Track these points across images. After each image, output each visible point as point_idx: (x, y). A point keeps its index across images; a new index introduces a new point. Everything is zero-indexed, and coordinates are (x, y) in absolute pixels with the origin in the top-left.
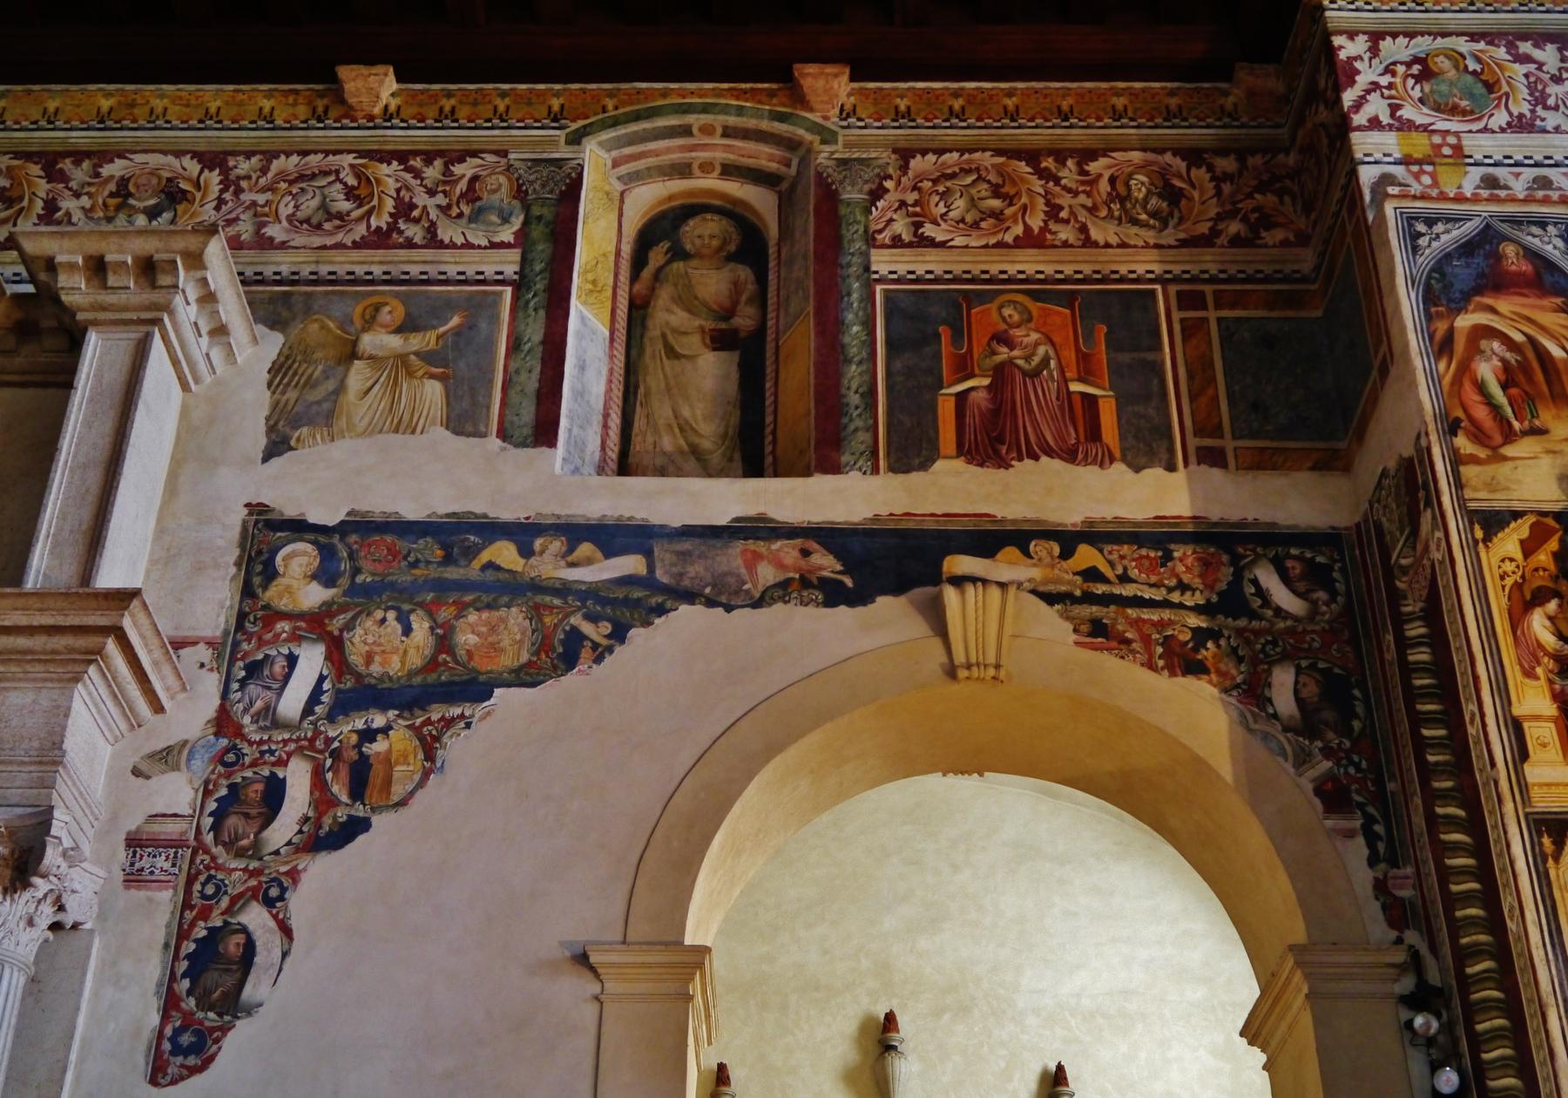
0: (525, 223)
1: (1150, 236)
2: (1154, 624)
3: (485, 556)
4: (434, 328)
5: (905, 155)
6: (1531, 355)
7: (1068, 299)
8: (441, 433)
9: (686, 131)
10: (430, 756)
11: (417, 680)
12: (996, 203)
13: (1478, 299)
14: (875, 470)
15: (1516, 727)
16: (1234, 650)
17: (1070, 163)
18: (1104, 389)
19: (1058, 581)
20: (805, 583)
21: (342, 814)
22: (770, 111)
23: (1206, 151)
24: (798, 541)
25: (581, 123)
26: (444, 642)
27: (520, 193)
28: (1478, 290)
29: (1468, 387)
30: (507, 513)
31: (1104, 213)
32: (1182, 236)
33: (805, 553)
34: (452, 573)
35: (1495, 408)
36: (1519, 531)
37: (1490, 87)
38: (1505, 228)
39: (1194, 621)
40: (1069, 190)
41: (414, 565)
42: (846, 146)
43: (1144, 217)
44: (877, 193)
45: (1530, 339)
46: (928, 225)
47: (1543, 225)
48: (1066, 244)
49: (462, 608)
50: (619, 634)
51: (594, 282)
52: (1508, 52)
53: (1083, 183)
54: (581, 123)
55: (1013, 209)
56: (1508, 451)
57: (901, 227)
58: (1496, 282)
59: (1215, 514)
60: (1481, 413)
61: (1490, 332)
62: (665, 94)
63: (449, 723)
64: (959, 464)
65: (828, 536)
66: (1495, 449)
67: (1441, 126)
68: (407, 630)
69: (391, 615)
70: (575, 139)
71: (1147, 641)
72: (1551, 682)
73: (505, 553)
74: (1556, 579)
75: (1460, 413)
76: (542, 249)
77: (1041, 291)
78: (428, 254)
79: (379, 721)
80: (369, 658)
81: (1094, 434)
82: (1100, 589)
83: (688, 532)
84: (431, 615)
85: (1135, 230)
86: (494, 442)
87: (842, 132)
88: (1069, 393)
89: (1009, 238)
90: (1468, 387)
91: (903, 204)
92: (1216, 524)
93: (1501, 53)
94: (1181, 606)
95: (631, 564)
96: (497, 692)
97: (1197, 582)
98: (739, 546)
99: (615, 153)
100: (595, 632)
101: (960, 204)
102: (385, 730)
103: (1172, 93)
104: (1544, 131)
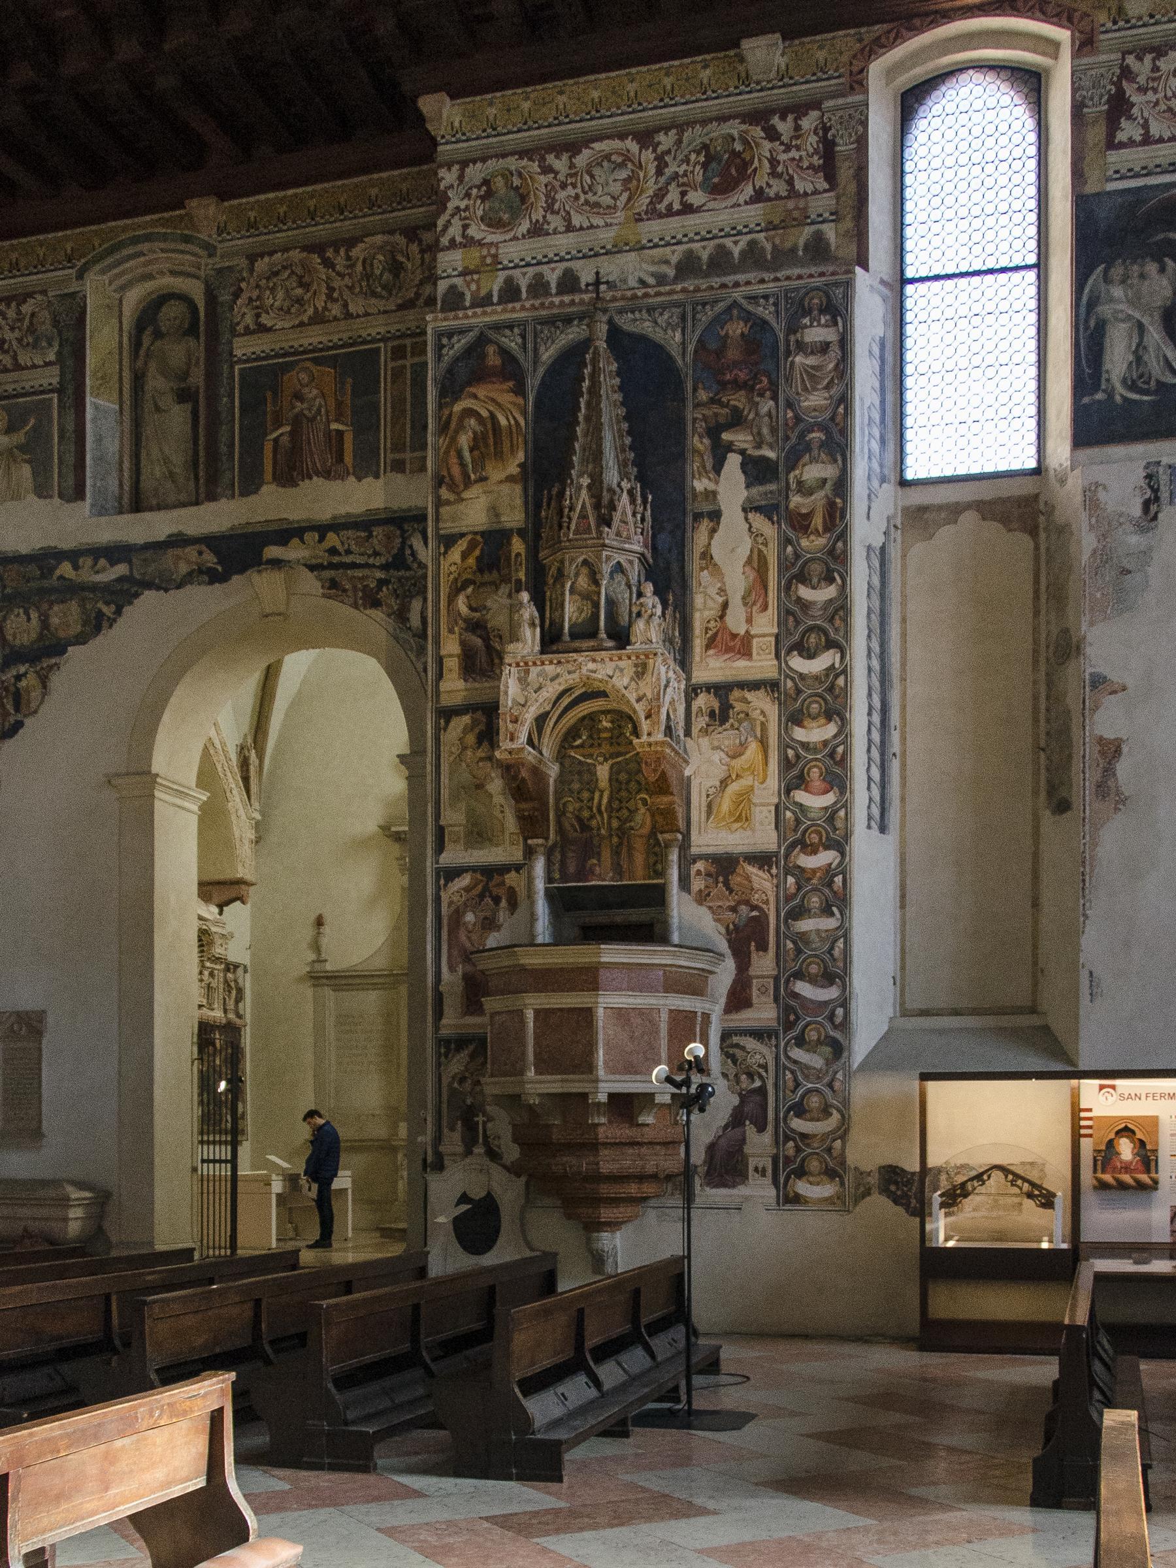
0: (61, 345)
1: (381, 304)
2: (360, 579)
3: (58, 572)
4: (22, 428)
5: (252, 258)
6: (489, 426)
7: (333, 361)
8: (32, 498)
10: (45, 687)
11: (35, 646)
12: (299, 291)
14: (233, 497)
15: (440, 661)
16: (395, 590)
17: (342, 251)
18: (346, 425)
19: (316, 557)
20: (200, 571)
21: (12, 720)
22: (181, 235)
23: (417, 227)
24: (197, 547)
25: (83, 261)
26: (45, 623)
27: (56, 323)
28: (469, 383)
29: (453, 453)
30: (66, 545)
31: (357, 290)
32: (400, 301)
33: (200, 553)
34: (46, 583)
35: (463, 465)
36: (462, 545)
37: (523, 198)
38: (492, 334)
39: (380, 575)
40: (339, 274)
41: (28, 581)
42: (222, 257)
43: (379, 289)
44: (237, 294)
45: (493, 416)
46: (264, 315)
47: (511, 328)
48: (336, 319)
49: (51, 604)
50: (119, 612)
51: (102, 378)
52: (540, 166)
53: (348, 267)
54: (83, 261)
55: (309, 294)
56: (465, 495)
57: (249, 320)
58: (480, 375)
59: (395, 506)
60: (456, 471)
61: (469, 412)
62: (124, 229)
63: (51, 668)
64: (273, 487)
65: (210, 541)
66: (458, 494)
67: (490, 238)
68: (29, 619)
69: (21, 611)
70: (80, 276)
71: (355, 588)
72: (460, 634)
73: (65, 569)
74: (474, 573)
75: (445, 473)
76: (70, 362)
77: (320, 357)
78: (14, 375)
79: (22, 669)
80: (15, 637)
81: (340, 459)
82: (336, 559)
83: (147, 546)
84: (38, 608)
85: (373, 301)
86: (57, 501)
87: (219, 246)
88: (330, 431)
89: (305, 319)
90: (453, 453)
91: (250, 299)
92: (395, 512)
93: (535, 167)
94: (374, 566)
95: (121, 569)
96: (69, 648)
97: (383, 550)
98: (170, 552)
100: (108, 610)
101: (280, 295)
102: (25, 674)
103: (404, 179)
104: (548, 234)
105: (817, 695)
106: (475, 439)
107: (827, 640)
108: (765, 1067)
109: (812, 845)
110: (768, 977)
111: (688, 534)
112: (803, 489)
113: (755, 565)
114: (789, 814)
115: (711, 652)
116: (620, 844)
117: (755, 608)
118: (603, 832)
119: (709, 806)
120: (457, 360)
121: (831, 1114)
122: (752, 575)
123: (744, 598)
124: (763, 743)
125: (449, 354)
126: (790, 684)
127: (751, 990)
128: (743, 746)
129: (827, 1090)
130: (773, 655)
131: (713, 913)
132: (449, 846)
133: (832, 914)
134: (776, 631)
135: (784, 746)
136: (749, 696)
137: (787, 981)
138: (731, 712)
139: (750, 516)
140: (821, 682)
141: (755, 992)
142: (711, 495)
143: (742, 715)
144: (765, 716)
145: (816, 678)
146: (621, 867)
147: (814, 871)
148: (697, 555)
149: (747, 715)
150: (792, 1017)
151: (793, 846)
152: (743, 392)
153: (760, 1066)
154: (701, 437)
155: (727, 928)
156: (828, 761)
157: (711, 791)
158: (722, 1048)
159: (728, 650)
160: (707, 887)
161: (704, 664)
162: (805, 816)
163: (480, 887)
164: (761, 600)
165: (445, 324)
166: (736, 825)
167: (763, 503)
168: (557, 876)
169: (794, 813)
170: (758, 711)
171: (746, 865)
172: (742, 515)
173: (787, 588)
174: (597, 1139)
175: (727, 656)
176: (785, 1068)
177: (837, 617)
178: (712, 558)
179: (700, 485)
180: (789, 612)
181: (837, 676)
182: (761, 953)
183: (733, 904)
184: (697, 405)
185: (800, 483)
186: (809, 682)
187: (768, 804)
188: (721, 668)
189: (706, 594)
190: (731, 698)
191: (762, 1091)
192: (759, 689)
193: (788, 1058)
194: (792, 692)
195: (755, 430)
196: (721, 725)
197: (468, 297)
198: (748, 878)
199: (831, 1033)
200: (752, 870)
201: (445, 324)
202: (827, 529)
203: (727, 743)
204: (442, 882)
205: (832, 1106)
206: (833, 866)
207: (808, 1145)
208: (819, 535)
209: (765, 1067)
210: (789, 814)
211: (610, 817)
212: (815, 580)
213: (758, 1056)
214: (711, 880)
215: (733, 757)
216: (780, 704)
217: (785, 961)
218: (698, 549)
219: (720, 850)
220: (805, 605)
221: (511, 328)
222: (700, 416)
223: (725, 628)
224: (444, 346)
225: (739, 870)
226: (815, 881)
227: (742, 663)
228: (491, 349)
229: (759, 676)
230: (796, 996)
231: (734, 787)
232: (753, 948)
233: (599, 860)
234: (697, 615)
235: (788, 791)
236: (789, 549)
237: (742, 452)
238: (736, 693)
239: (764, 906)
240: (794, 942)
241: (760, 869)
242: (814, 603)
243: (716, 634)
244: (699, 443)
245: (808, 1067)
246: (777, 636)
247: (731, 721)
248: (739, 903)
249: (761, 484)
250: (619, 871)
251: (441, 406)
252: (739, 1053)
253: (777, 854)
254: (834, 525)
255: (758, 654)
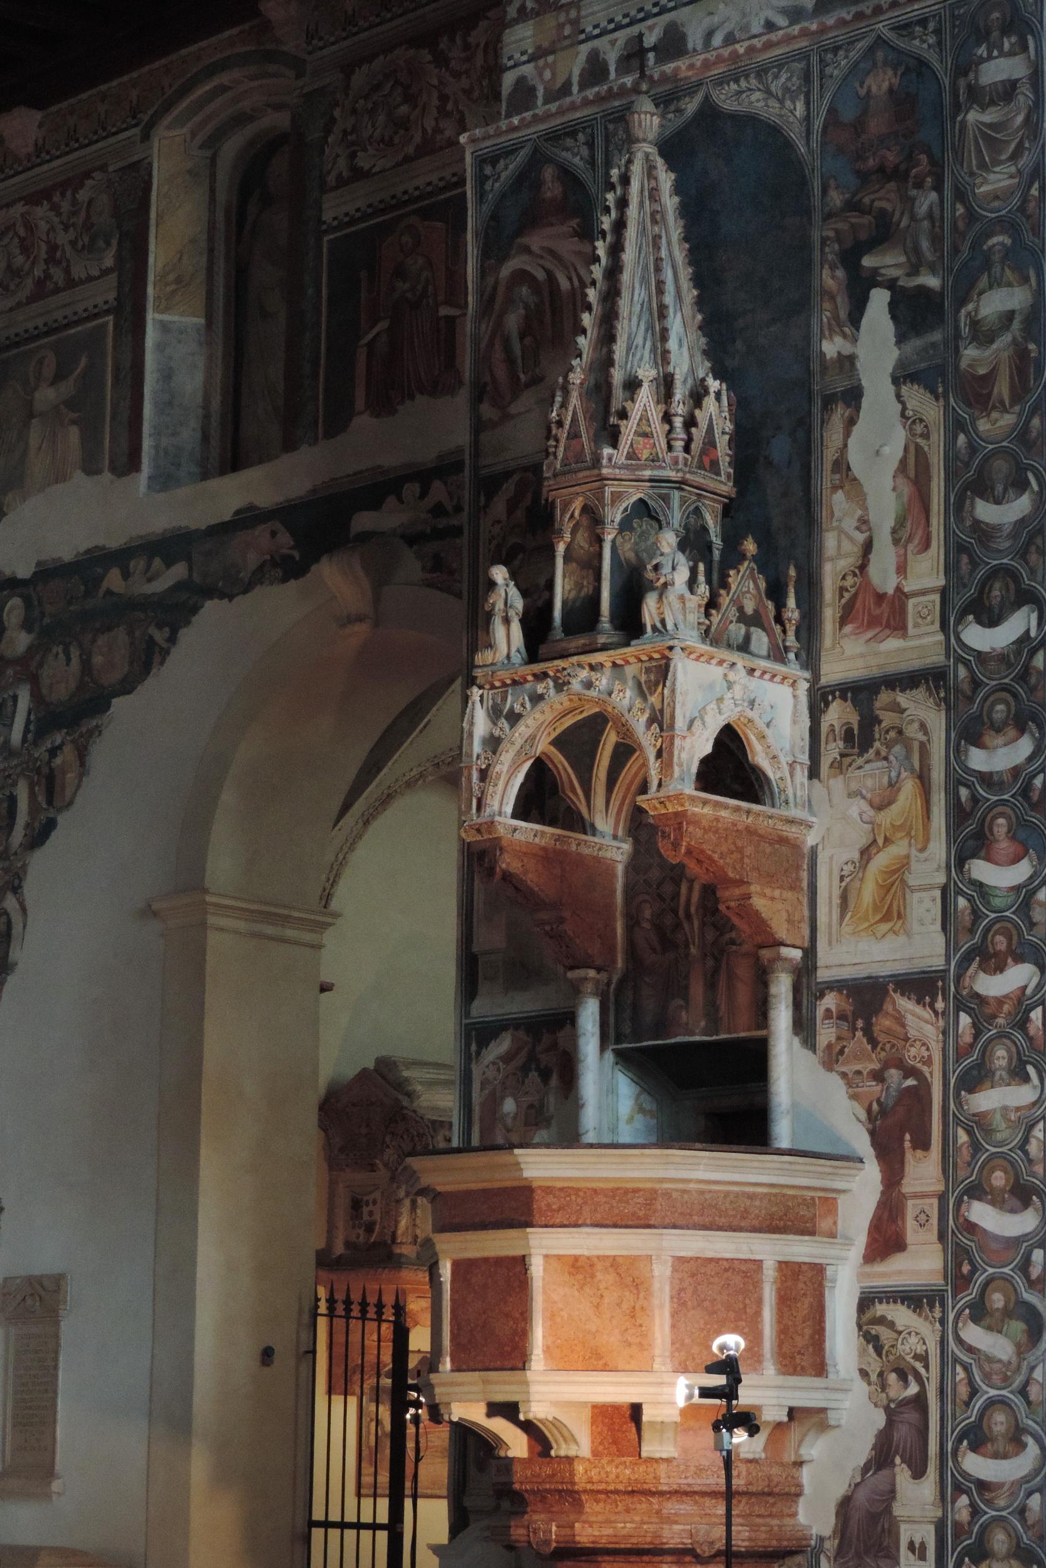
9: (223, 89)
13: (519, 240)
28: (520, 231)
29: (498, 347)
45: (551, 277)
56: (513, 409)
58: (532, 219)
75: (488, 379)
90: (498, 347)
99: (189, 125)
105: (1004, 688)
106: (527, 317)
107: (1018, 590)
108: (924, 1358)
109: (996, 954)
110: (932, 1196)
111: (816, 434)
112: (983, 335)
113: (912, 474)
114: (962, 902)
115: (848, 629)
116: (716, 971)
117: (911, 547)
118: (693, 950)
119: (844, 898)
120: (503, 196)
121: (1024, 1446)
122: (906, 489)
123: (894, 531)
124: (923, 778)
125: (494, 188)
126: (962, 672)
127: (903, 1219)
128: (894, 786)
129: (1017, 1401)
130: (937, 625)
131: (849, 1085)
132: (483, 988)
133: (1026, 1079)
134: (941, 582)
135: (954, 782)
136: (903, 699)
137: (959, 1202)
138: (876, 729)
139: (904, 389)
140: (1010, 665)
141: (910, 1224)
142: (847, 362)
143: (892, 734)
144: (926, 733)
145: (1003, 658)
146: (717, 1010)
147: (1000, 1001)
148: (828, 466)
149: (900, 732)
150: (966, 1268)
151: (966, 960)
152: (892, 185)
153: (917, 1357)
154: (833, 268)
155: (869, 1111)
156: (1019, 802)
157: (848, 869)
158: (860, 1327)
159: (873, 622)
160: (839, 1038)
161: (838, 650)
162: (988, 905)
163: (524, 1053)
164: (920, 533)
165: (488, 143)
166: (884, 927)
167: (923, 365)
168: (627, 1029)
169: (970, 899)
170: (916, 725)
171: (897, 997)
172: (892, 388)
173: (957, 507)
174: (573, 1483)
175: (869, 634)
176: (956, 1360)
177: (1033, 549)
178: (849, 468)
179: (831, 348)
180: (961, 548)
181: (1033, 652)
182: (919, 1153)
183: (876, 1066)
184: (828, 216)
185: (975, 324)
186: (992, 665)
187: (931, 888)
188: (862, 655)
189: (841, 531)
190: (877, 704)
191: (919, 1402)
192: (917, 687)
193: (960, 1341)
194: (966, 687)
195: (909, 244)
196: (860, 755)
197: (540, 93)
198: (900, 1020)
199: (1027, 1296)
200: (906, 1005)
201: (488, 143)
202: (1016, 398)
203: (869, 782)
204: (474, 1047)
205: (1026, 1431)
206: (1029, 991)
207: (989, 1503)
208: (1005, 411)
209: (924, 1358)
210: (962, 902)
211: (703, 924)
212: (999, 488)
213: (913, 1340)
214: (845, 1025)
215: (880, 808)
216: (948, 710)
217: (955, 1165)
218: (830, 455)
219: (861, 972)
220: (984, 533)
221: (573, 134)
222: (831, 234)
223: (867, 584)
224: (487, 178)
225: (888, 1007)
226: (1000, 1021)
227: (893, 643)
228: (548, 173)
229: (916, 664)
230: (971, 1228)
231: (881, 860)
232: (907, 1144)
233: (686, 999)
234: (828, 568)
235: (961, 862)
236: (962, 439)
237: (891, 285)
238: (884, 697)
239: (925, 1069)
240: (970, 1132)
241: (918, 1002)
242: (997, 528)
243: (855, 596)
244: (831, 279)
245: (990, 1359)
246: (944, 592)
247: (877, 744)
248: (886, 1065)
249: (918, 334)
250: (714, 1021)
251: (483, 273)
252: (885, 1333)
253: (943, 974)
254: (1026, 390)
255: (916, 625)
